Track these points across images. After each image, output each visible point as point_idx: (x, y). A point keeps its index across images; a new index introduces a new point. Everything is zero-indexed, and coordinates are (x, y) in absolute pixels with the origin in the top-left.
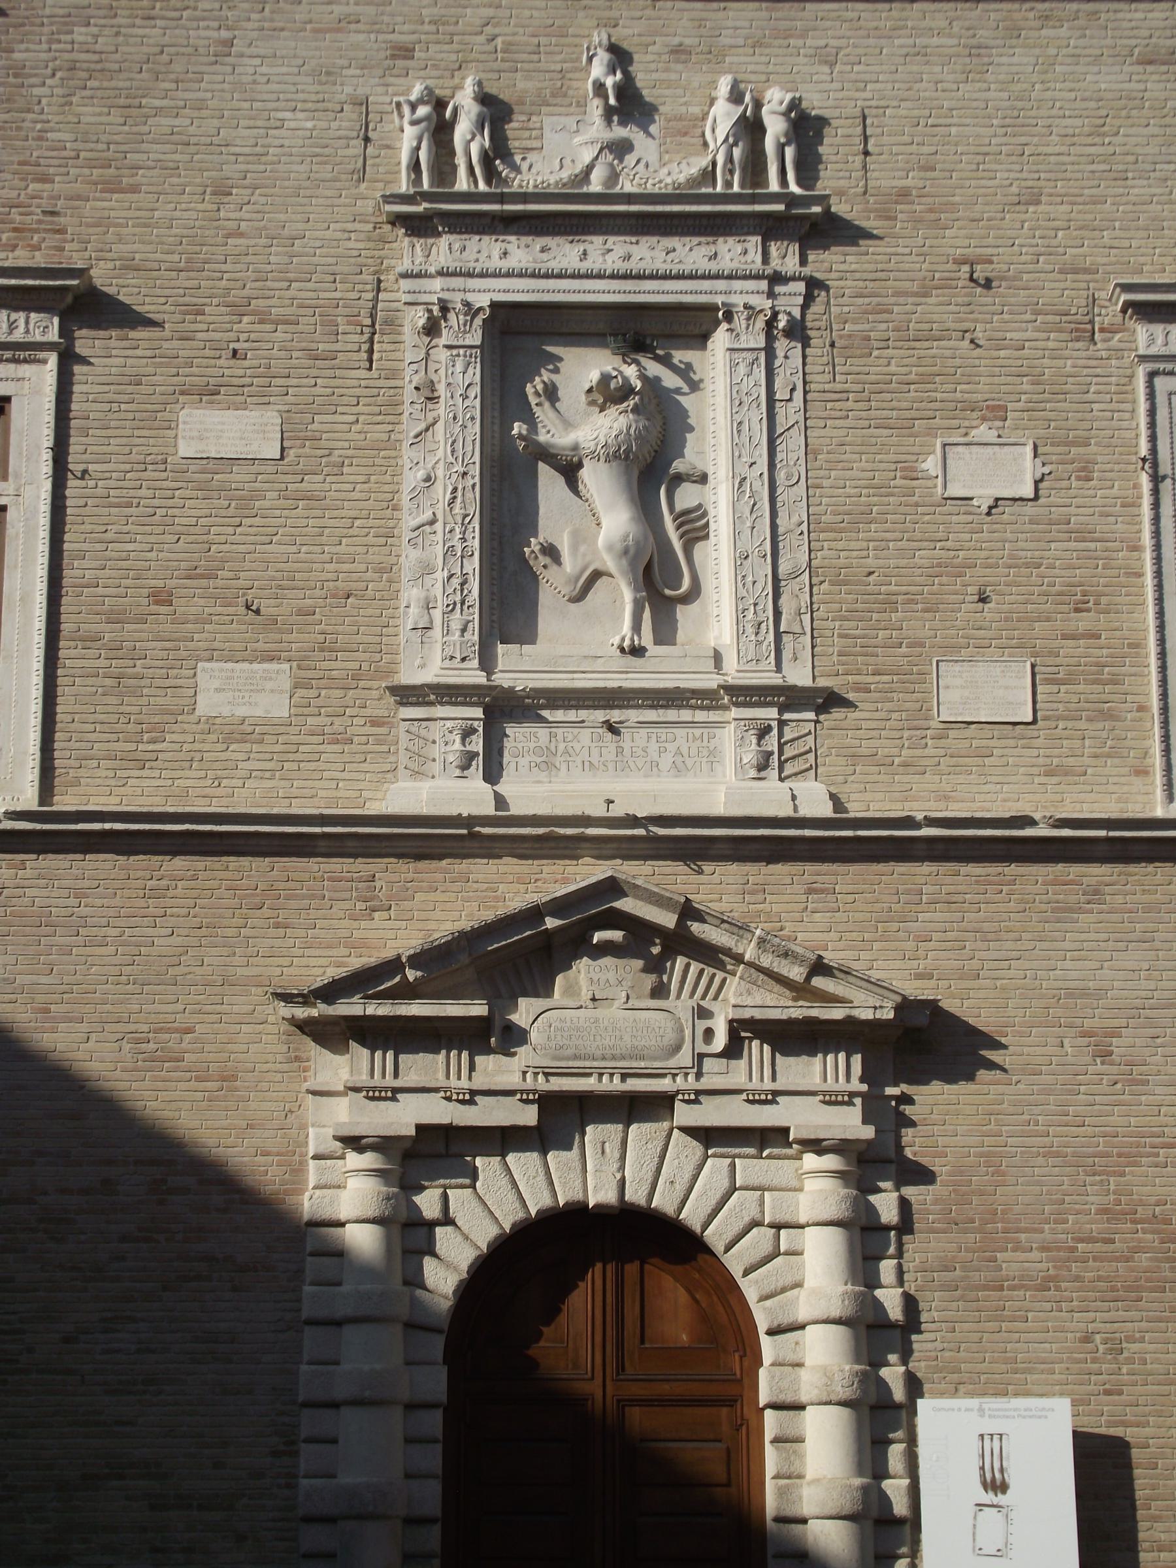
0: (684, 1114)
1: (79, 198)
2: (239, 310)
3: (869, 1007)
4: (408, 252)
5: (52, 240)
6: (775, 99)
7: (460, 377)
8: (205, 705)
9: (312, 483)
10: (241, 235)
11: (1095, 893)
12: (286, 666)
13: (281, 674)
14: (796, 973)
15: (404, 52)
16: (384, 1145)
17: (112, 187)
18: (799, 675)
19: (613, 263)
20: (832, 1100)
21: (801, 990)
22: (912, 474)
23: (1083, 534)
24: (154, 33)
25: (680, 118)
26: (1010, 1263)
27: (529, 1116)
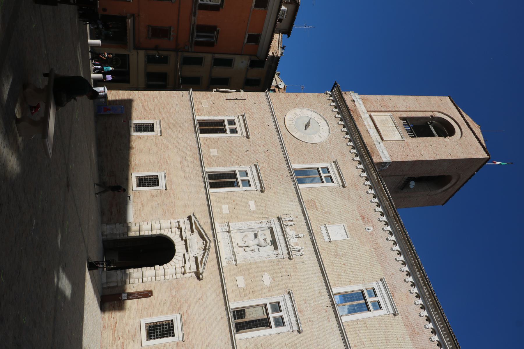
0: (186, 254)
3: (201, 270)
4: (276, 220)
6: (303, 253)
7: (264, 225)
8: (223, 206)
12: (228, 213)
13: (228, 213)
14: (203, 262)
15: (297, 217)
16: (179, 225)
17: (275, 193)
19: (280, 238)
20: (190, 268)
21: (201, 263)
22: (264, 271)
26: (173, 291)
27: (184, 238)
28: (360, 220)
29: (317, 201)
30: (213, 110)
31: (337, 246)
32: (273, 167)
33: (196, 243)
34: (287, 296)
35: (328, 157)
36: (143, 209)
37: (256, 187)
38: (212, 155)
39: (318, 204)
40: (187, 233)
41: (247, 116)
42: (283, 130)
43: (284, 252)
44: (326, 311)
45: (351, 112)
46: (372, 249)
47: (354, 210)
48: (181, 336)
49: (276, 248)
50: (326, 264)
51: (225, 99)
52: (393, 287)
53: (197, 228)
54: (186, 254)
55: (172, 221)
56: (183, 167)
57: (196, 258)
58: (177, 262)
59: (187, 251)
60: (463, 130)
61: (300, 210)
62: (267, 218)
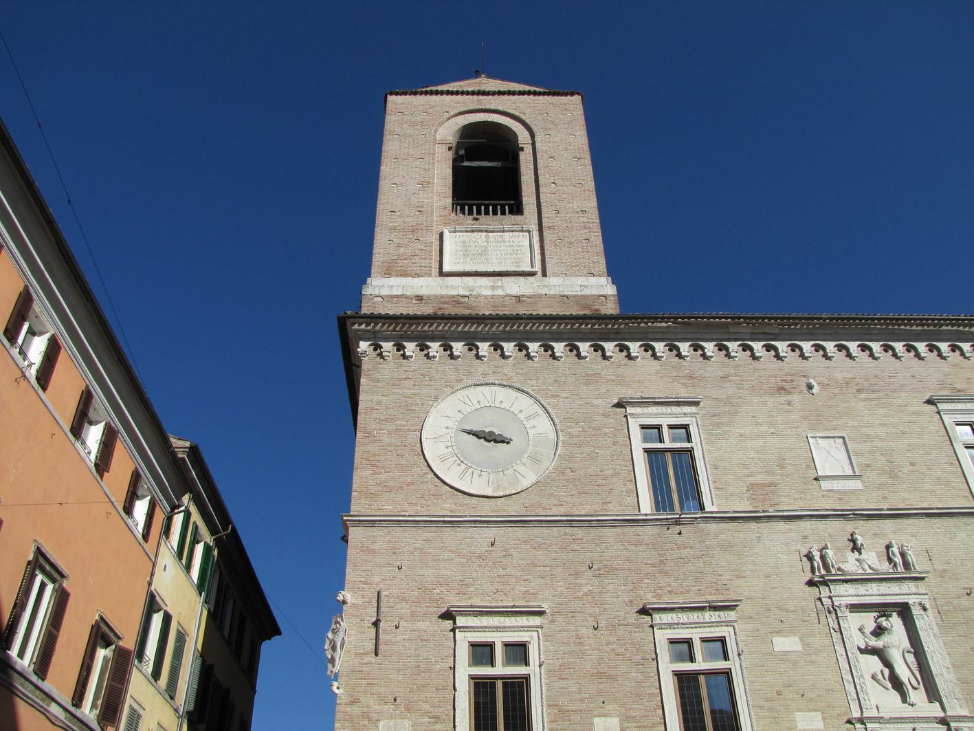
1: (731, 580)
9: (813, 658)
10: (776, 588)
17: (738, 577)
24: (741, 535)
25: (880, 552)
28: (789, 397)
29: (752, 480)
30: (427, 707)
31: (868, 466)
32: (653, 565)
35: (607, 416)
39: (758, 479)
41: (454, 601)
42: (512, 509)
43: (914, 590)
45: (439, 313)
46: (863, 396)
47: (764, 404)
50: (916, 501)
51: (372, 658)
52: (942, 384)
60: (500, 108)
61: (782, 526)
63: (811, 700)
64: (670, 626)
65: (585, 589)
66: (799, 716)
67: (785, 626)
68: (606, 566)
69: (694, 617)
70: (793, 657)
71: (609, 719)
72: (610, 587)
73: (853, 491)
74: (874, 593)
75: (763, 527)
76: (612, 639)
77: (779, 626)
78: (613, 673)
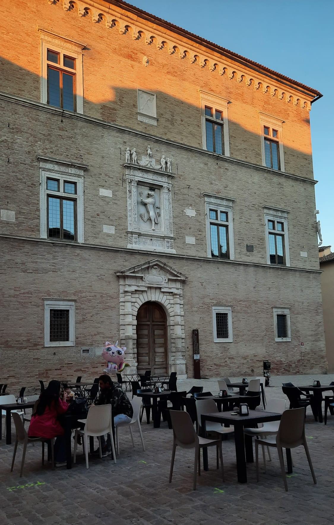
2: (106, 175)
5: (81, 160)
9: (116, 202)
11: (201, 266)
14: (176, 273)
18: (172, 236)
19: (151, 178)
22: (183, 211)
23: (200, 222)
27: (146, 289)
33: (155, 277)
34: (206, 199)
36: (103, 333)
37: (79, 176)
38: (14, 221)
40: (142, 285)
44: (220, 167)
46: (169, 76)
48: (228, 308)
49: (160, 187)
53: (137, 272)
54: (162, 290)
55: (122, 300)
56: (36, 271)
57: (169, 280)
58: (168, 301)
59: (160, 288)
62: (124, 181)
63: (112, 220)
64: (49, 170)
65: (3, 138)
66: (105, 227)
67: (107, 184)
68: (17, 128)
69: (63, 169)
70: (107, 199)
71: (10, 212)
72: (18, 141)
73: (152, 126)
74: (149, 178)
75: (106, 133)
76: (15, 170)
77: (104, 183)
78: (14, 188)
